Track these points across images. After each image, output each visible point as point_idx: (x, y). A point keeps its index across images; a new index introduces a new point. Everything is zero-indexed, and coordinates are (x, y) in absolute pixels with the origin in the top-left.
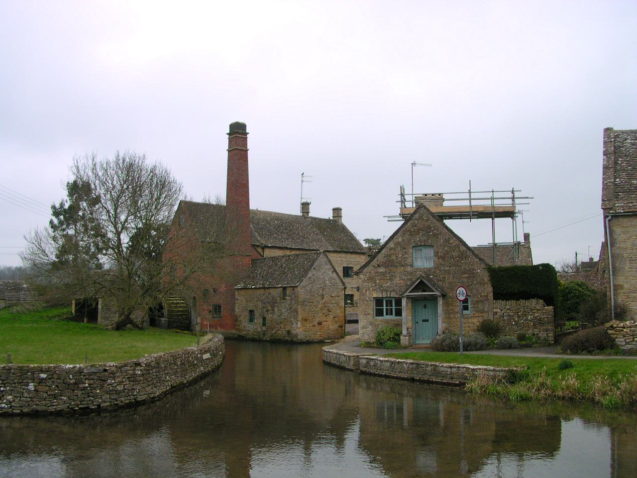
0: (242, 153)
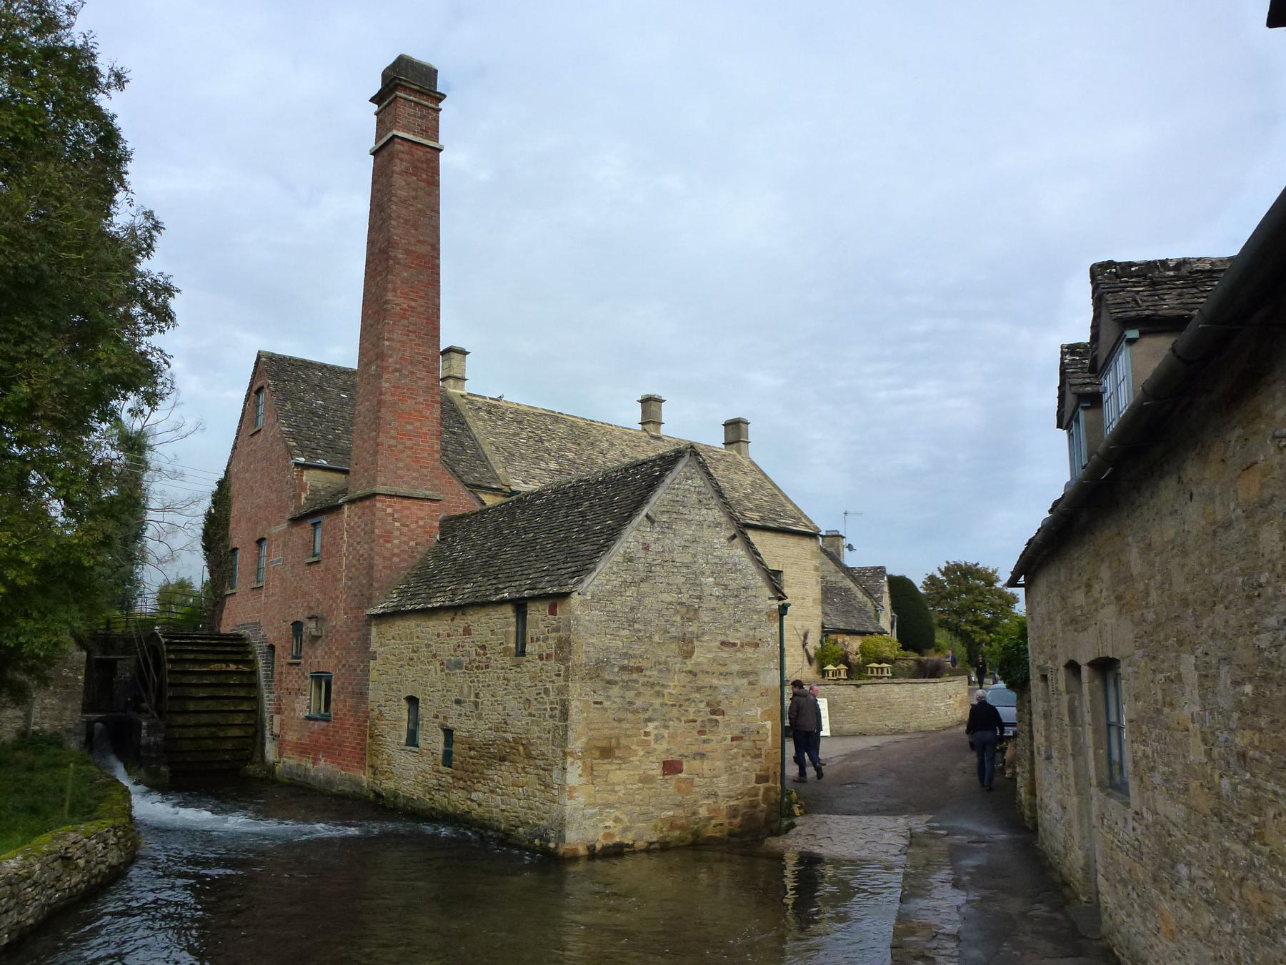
0: (419, 153)
